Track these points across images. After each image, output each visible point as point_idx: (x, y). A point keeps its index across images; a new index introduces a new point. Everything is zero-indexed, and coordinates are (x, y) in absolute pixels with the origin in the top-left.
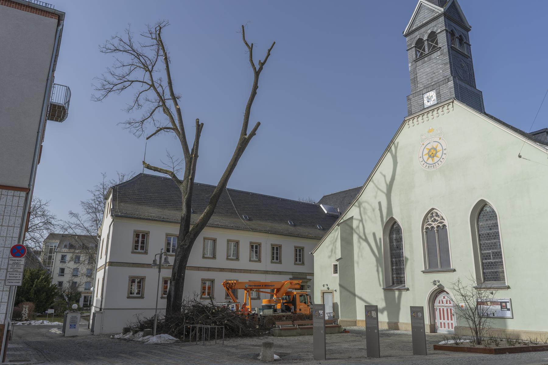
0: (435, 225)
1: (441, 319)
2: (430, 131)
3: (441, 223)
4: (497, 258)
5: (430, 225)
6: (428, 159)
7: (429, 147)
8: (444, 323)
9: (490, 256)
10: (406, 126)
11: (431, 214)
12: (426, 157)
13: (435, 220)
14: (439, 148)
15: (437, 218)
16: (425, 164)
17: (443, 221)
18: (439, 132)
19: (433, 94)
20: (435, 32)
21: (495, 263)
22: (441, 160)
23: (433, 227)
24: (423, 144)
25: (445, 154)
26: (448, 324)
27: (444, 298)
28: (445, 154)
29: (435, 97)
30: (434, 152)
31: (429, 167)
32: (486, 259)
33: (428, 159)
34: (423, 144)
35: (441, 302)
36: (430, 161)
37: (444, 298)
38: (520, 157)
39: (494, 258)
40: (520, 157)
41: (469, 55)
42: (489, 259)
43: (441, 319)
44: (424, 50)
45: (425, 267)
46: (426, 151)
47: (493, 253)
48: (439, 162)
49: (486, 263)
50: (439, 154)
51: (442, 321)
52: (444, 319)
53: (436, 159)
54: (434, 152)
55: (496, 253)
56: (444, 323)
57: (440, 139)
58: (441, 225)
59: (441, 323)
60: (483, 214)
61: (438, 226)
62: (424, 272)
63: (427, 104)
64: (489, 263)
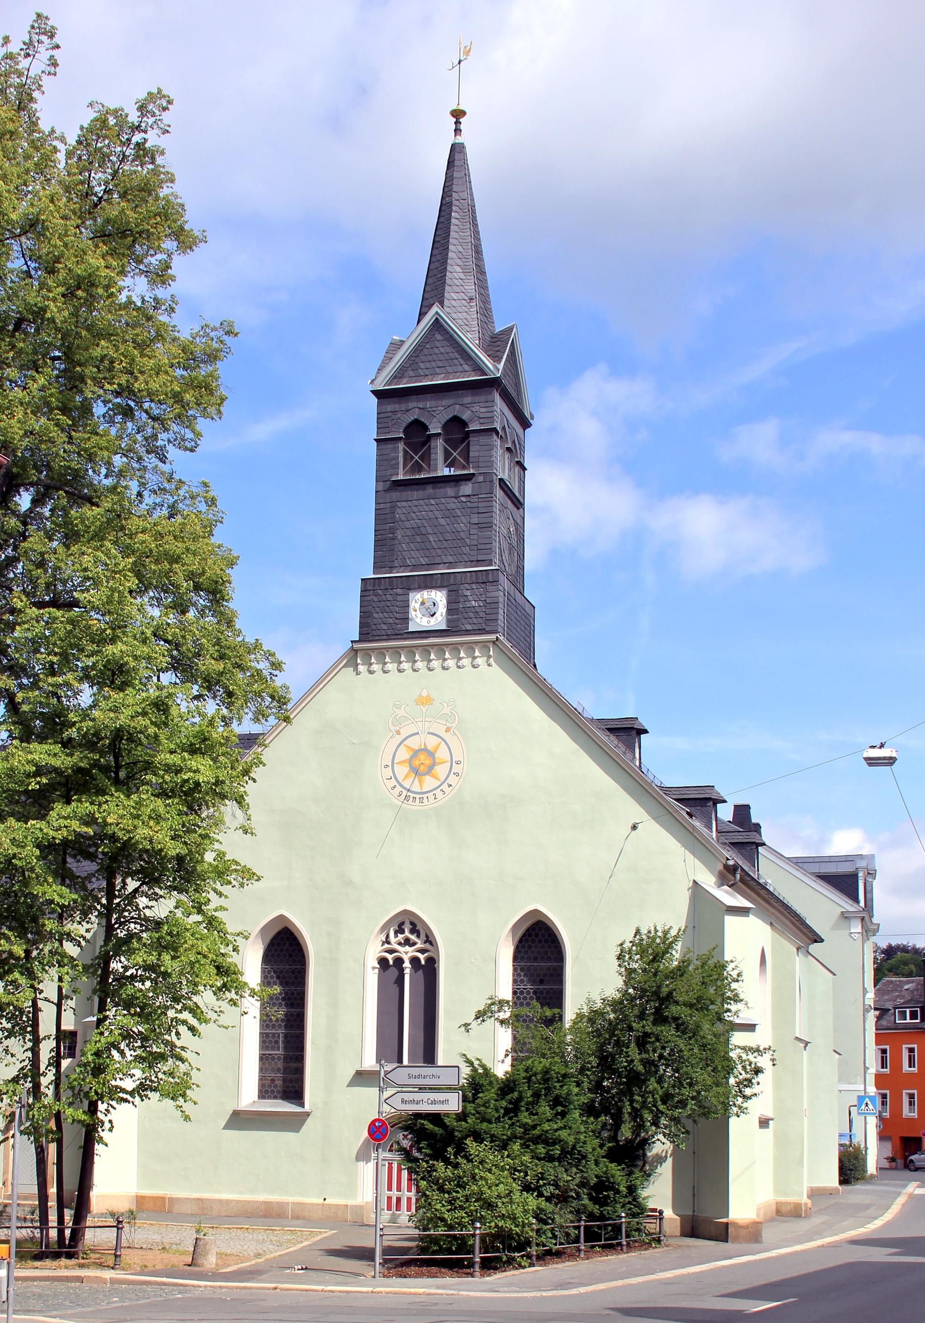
0: (407, 953)
1: (390, 1189)
5: (391, 951)
7: (414, 743)
8: (399, 1200)
12: (402, 771)
13: (407, 942)
14: (442, 754)
15: (413, 937)
16: (399, 788)
17: (427, 946)
18: (446, 710)
19: (439, 597)
20: (464, 424)
23: (399, 961)
24: (398, 733)
25: (457, 774)
28: (457, 774)
29: (442, 609)
34: (398, 733)
40: (634, 827)
41: (521, 500)
43: (390, 1189)
46: (403, 754)
48: (438, 792)
50: (441, 771)
51: (394, 1193)
53: (429, 783)
54: (428, 762)
56: (399, 1200)
57: (448, 730)
58: (422, 957)
59: (389, 1199)
63: (419, 621)
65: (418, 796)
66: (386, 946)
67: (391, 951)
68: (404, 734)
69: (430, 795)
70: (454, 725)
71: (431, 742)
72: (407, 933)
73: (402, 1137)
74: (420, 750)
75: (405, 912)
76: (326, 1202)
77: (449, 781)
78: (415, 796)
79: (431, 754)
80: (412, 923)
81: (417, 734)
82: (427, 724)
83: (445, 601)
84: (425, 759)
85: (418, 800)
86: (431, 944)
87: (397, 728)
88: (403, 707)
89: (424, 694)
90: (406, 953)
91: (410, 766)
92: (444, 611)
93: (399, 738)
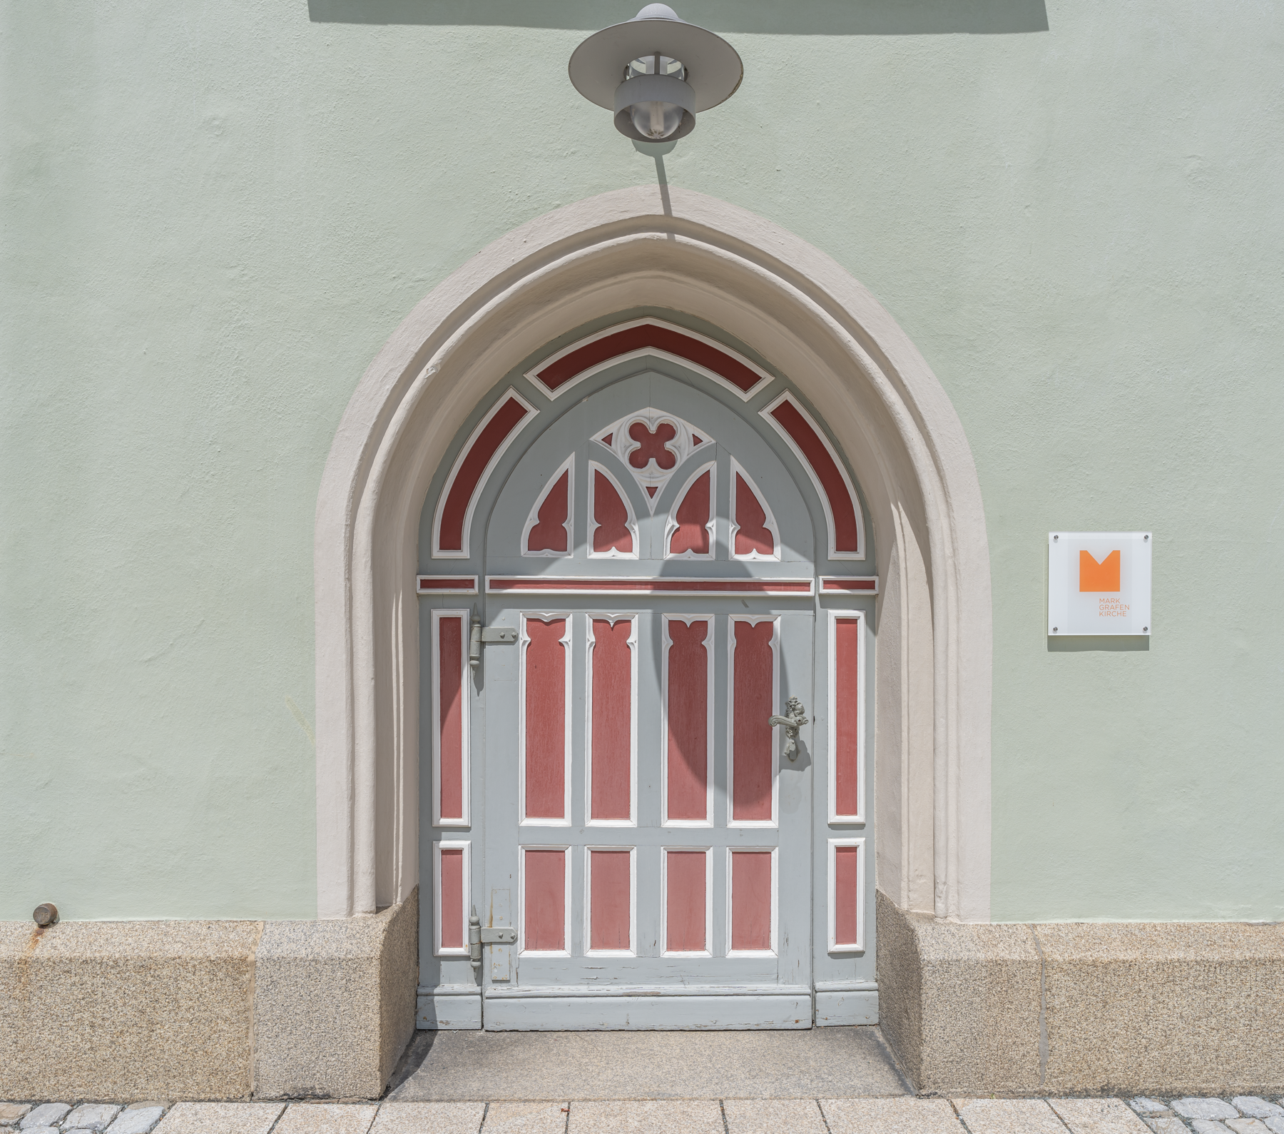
1: (545, 796)
8: (610, 866)
26: (686, 865)
27: (652, 445)
37: (652, 445)
43: (545, 796)
51: (576, 825)
52: (611, 798)
56: (610, 866)
59: (545, 864)
73: (624, 446)
76: (56, 943)
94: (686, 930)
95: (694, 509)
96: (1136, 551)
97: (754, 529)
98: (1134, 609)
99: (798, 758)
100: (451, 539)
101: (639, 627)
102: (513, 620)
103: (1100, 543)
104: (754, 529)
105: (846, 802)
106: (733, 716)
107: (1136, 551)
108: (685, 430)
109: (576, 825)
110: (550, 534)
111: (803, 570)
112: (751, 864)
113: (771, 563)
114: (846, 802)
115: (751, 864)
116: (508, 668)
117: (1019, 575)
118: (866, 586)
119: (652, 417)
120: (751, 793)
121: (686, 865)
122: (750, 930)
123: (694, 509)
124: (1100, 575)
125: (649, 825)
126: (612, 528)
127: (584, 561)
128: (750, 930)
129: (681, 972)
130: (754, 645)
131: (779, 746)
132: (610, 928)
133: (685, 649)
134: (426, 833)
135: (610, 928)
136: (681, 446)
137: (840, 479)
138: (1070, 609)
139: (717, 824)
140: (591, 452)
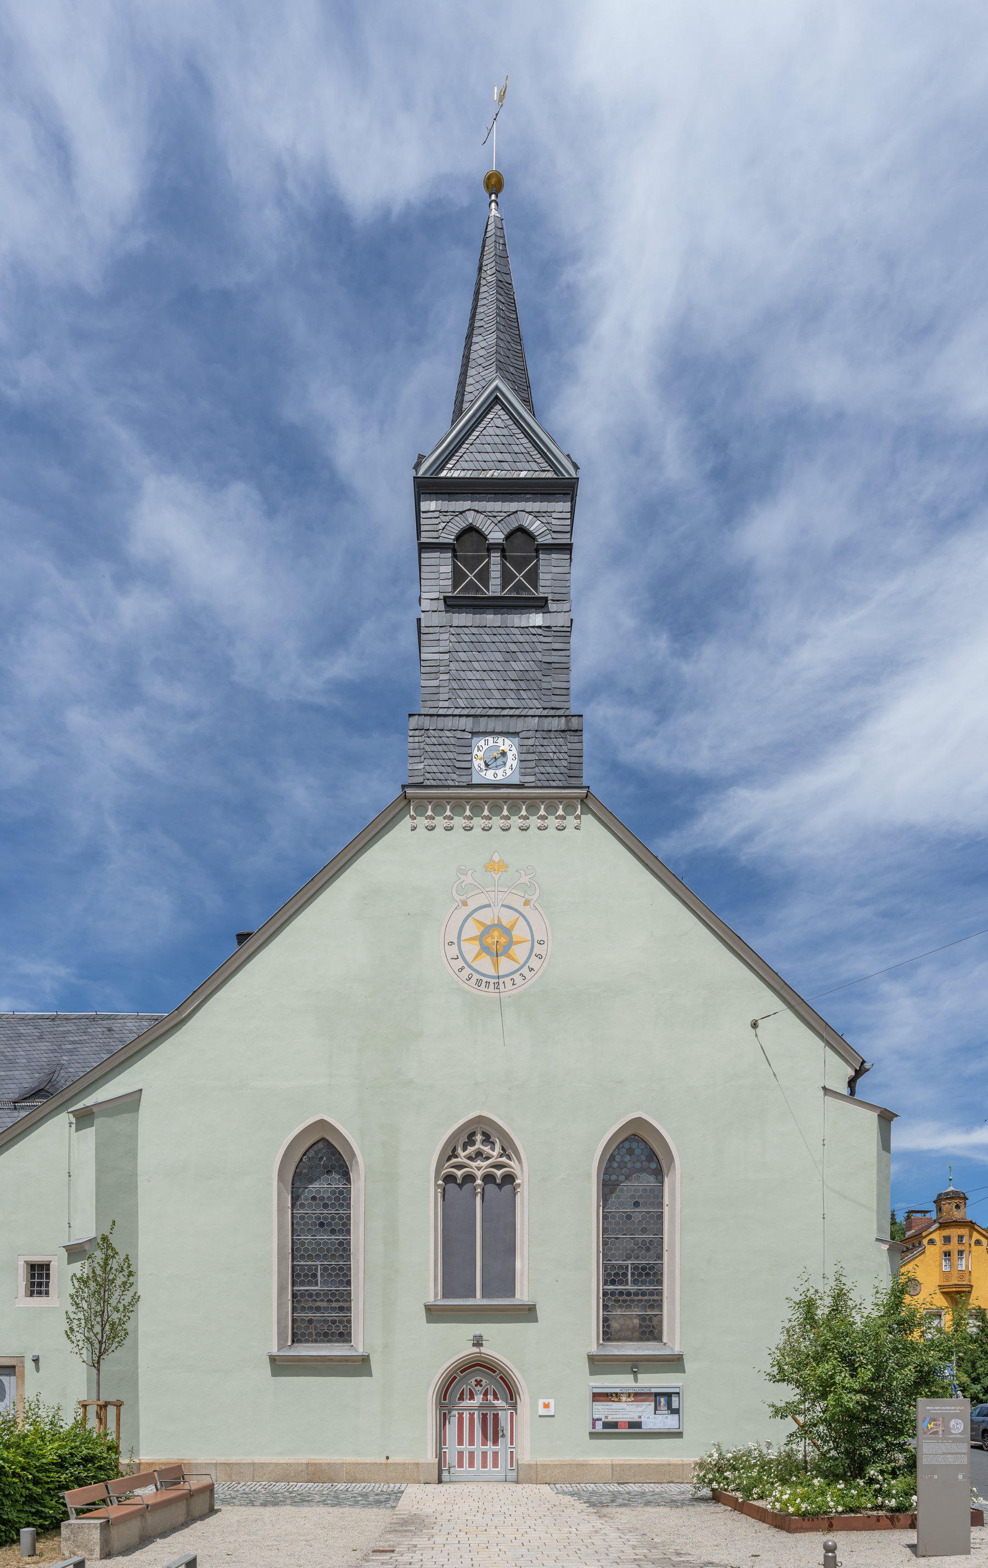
0: (479, 1168)
1: (460, 1442)
2: (490, 867)
3: (499, 1166)
4: (644, 1283)
5: (459, 1167)
6: (496, 965)
7: (486, 917)
8: (472, 1454)
9: (625, 1275)
10: (407, 822)
11: (479, 1133)
12: (471, 949)
13: (479, 1154)
14: (520, 931)
15: (487, 1149)
16: (467, 971)
17: (504, 1159)
18: (525, 879)
21: (636, 1294)
22: (525, 971)
23: (469, 1178)
24: (465, 903)
25: (539, 956)
26: (484, 1454)
28: (539, 956)
29: (512, 761)
30: (503, 940)
31: (479, 982)
32: (613, 1282)
33: (496, 965)
34: (465, 903)
35: (467, 1395)
36: (485, 965)
37: (479, 1383)
38: (755, 1025)
39: (635, 1282)
40: (755, 1025)
42: (621, 1283)
43: (460, 1442)
44: (484, 576)
45: (436, 1296)
46: (472, 930)
47: (635, 1268)
48: (517, 977)
49: (613, 1294)
50: (520, 952)
51: (466, 1447)
52: (472, 1442)
53: (506, 965)
54: (503, 940)
55: (644, 1269)
56: (472, 1454)
57: (527, 903)
59: (461, 1454)
60: (635, 1161)
61: (489, 1178)
62: (429, 1309)
64: (621, 1293)
65: (492, 981)
66: (454, 1160)
67: (459, 1167)
68: (473, 905)
69: (507, 980)
70: (535, 897)
71: (507, 917)
72: (478, 1145)
73: (474, 1383)
74: (493, 926)
75: (480, 1119)
77: (530, 964)
78: (488, 980)
79: (507, 931)
80: (484, 1134)
81: (489, 906)
82: (501, 895)
83: (515, 751)
84: (499, 937)
85: (492, 986)
86: (509, 1158)
87: (464, 898)
88: (470, 873)
89: (496, 858)
90: (479, 1168)
91: (481, 944)
92: (515, 763)
93: (466, 911)
94: (484, 1465)
95: (486, 1394)
96: (552, 1402)
97: (496, 1397)
98: (551, 1411)
99: (503, 1436)
100: (445, 1399)
101: (476, 1413)
102: (455, 1413)
103: (546, 1401)
104: (496, 1397)
105: (512, 1444)
106: (492, 1429)
107: (552, 1402)
108: (484, 1380)
109: (466, 1447)
110: (461, 1398)
111: (504, 1404)
112: (495, 1454)
113: (499, 1403)
114: (512, 1444)
115: (495, 1454)
116: (455, 1420)
117: (534, 1406)
118: (514, 1407)
119: (478, 1378)
120: (495, 1442)
121: (484, 1454)
122: (495, 1465)
123: (486, 1394)
124: (546, 1406)
125: (478, 1448)
126: (472, 1397)
127: (467, 1403)
128: (495, 1465)
129: (483, 1472)
130: (496, 1417)
131: (500, 1434)
132: (471, 1464)
133: (484, 1417)
134: (441, 1449)
135: (471, 1464)
136: (483, 1383)
137: (510, 1391)
138: (542, 1411)
139: (490, 1447)
140: (468, 1384)
